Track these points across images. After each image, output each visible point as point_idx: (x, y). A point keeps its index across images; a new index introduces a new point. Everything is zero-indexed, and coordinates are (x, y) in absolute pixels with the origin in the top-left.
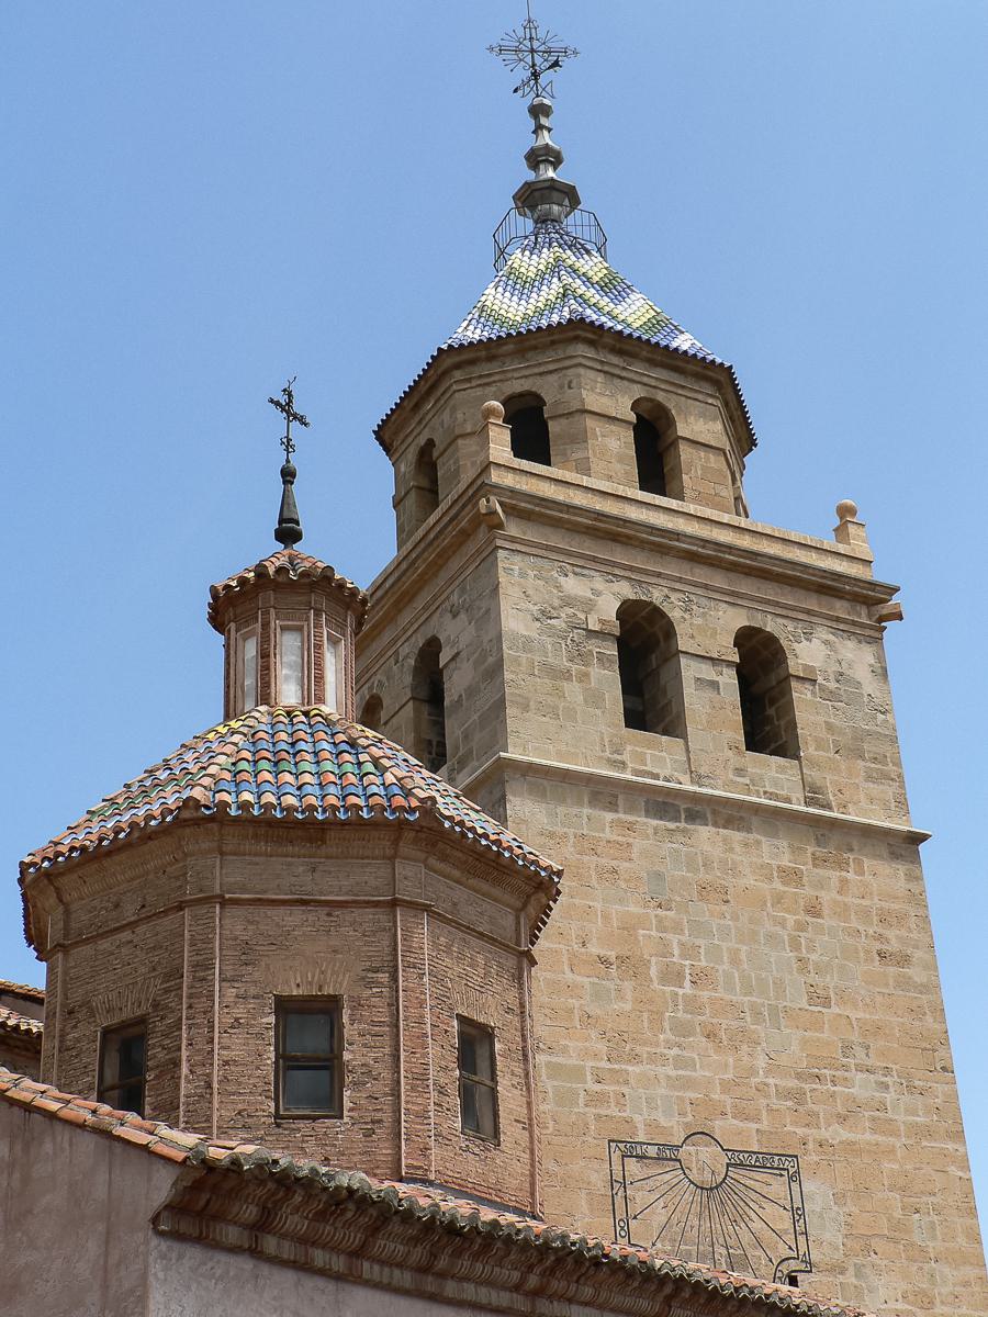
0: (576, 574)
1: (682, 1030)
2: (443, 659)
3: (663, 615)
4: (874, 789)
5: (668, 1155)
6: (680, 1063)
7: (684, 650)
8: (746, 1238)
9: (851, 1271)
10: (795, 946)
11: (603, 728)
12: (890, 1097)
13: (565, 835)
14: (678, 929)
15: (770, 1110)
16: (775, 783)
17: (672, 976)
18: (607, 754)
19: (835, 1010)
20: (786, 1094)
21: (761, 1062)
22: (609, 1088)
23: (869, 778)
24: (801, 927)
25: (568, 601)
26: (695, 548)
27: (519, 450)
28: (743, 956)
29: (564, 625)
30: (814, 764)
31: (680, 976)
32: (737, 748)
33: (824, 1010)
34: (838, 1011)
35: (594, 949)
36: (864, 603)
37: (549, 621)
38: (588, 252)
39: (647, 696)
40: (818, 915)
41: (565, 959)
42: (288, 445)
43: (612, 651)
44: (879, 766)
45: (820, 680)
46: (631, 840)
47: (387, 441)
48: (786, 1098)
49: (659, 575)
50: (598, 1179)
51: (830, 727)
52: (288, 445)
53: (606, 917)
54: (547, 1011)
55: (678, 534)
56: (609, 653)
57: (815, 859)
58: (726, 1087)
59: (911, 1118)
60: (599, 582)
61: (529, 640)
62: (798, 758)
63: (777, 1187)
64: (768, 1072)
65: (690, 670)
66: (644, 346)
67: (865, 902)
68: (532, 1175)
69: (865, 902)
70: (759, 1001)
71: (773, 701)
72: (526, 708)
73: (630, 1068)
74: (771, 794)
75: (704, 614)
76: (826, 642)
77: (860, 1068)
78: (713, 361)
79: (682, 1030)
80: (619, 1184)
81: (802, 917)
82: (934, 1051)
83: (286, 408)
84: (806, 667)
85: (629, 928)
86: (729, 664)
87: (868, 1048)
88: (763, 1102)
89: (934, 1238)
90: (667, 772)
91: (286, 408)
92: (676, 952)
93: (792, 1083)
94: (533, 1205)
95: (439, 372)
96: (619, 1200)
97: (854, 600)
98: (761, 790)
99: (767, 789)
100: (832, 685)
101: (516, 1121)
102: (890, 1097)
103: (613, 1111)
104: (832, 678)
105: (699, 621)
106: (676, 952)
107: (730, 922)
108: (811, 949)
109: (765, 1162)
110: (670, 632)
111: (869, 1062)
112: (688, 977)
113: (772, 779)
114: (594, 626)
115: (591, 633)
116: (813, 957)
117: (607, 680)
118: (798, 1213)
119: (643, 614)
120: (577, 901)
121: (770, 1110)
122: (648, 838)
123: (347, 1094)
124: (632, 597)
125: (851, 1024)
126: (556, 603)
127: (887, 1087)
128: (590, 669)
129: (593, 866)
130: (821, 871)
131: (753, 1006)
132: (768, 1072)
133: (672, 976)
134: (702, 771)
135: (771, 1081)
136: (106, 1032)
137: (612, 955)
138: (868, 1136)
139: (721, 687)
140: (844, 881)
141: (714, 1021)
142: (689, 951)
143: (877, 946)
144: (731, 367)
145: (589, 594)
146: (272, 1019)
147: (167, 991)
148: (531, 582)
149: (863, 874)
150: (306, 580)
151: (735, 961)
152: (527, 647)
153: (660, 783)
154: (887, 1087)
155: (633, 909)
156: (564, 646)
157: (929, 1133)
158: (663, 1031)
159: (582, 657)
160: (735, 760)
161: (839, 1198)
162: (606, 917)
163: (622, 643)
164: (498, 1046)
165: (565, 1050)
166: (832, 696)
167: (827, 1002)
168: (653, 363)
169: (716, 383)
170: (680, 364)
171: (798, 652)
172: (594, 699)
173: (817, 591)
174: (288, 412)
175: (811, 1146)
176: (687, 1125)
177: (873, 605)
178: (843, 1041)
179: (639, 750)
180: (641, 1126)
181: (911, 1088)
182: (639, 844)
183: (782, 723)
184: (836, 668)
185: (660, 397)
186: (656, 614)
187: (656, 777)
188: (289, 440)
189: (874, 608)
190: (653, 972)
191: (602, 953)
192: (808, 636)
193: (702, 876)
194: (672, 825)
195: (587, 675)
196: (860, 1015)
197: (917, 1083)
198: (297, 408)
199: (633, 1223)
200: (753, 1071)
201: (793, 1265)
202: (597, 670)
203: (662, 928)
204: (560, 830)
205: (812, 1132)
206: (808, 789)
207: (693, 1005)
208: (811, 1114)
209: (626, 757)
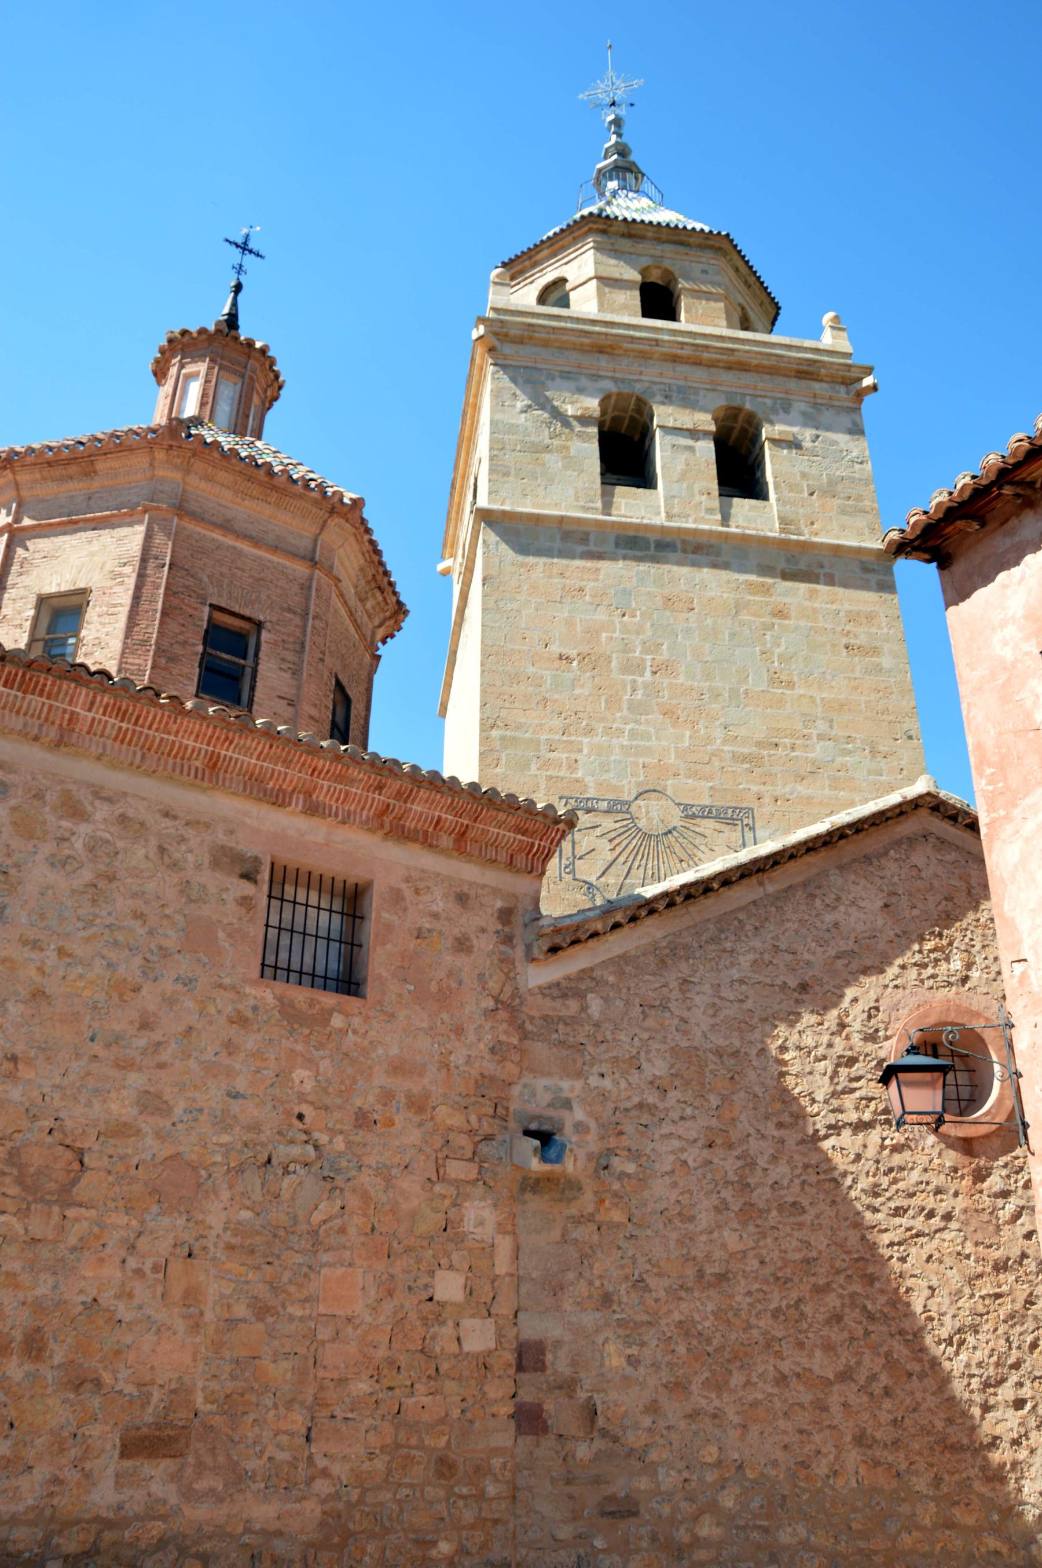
0: (561, 377)
1: (637, 709)
5: (618, 807)
6: (633, 735)
17: (633, 667)
19: (799, 691)
20: (745, 759)
21: (718, 733)
23: (843, 512)
33: (788, 692)
34: (802, 692)
35: (555, 649)
36: (843, 383)
42: (240, 269)
43: (594, 430)
48: (743, 762)
51: (804, 475)
52: (240, 269)
53: (570, 623)
64: (725, 742)
66: (650, 228)
73: (586, 740)
81: (767, 619)
83: (244, 247)
85: (592, 633)
86: (706, 434)
87: (831, 721)
91: (244, 247)
92: (639, 649)
101: (280, 697)
111: (834, 732)
112: (649, 669)
119: (632, 407)
125: (814, 702)
131: (710, 689)
132: (725, 742)
133: (633, 667)
135: (726, 748)
137: (573, 653)
141: (674, 702)
143: (844, 641)
144: (728, 235)
146: (31, 613)
150: (204, 337)
158: (620, 710)
164: (265, 635)
167: (790, 684)
168: (659, 240)
169: (718, 250)
170: (683, 238)
172: (571, 463)
174: (244, 249)
175: (766, 800)
176: (638, 784)
180: (591, 784)
188: (241, 266)
189: (851, 387)
190: (614, 664)
191: (565, 651)
195: (567, 448)
196: (825, 695)
197: (881, 748)
198: (251, 246)
199: (577, 862)
200: (709, 740)
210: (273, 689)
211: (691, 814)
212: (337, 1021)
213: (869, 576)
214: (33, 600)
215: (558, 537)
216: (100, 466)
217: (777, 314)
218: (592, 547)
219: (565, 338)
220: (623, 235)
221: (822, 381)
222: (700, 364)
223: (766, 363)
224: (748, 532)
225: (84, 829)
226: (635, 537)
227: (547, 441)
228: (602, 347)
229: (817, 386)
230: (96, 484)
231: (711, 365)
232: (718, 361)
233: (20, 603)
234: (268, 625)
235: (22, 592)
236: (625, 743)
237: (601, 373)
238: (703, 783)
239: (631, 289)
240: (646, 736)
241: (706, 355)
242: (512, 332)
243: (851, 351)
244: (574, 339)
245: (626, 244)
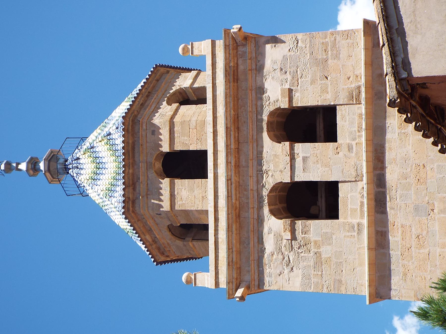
4: (344, 54)
7: (290, 179)
13: (403, 266)
18: (355, 234)
23: (337, 57)
26: (233, 168)
29: (292, 253)
32: (337, 148)
36: (237, 49)
37: (291, 262)
43: (299, 224)
44: (329, 48)
45: (287, 86)
46: (400, 226)
51: (313, 82)
55: (228, 180)
56: (301, 227)
61: (304, 276)
66: (127, 172)
74: (359, 127)
78: (123, 129)
84: (283, 96)
86: (292, 148)
90: (359, 196)
97: (237, 56)
98: (358, 134)
99: (356, 129)
104: (285, 77)
107: (435, 165)
114: (288, 236)
115: (294, 238)
120: (438, 264)
128: (312, 240)
129: (417, 251)
134: (354, 174)
139: (305, 155)
145: (272, 235)
153: (365, 201)
156: (302, 254)
166: (295, 79)
171: (275, 99)
173: (237, 82)
177: (237, 43)
179: (349, 212)
195: (316, 242)
202: (311, 235)
206: (351, 102)
215: (382, 251)
217: (162, 66)
219: (234, 241)
220: (134, 189)
221: (237, 64)
222: (238, 149)
223: (232, 105)
224: (364, 126)
226: (376, 201)
227: (312, 254)
228: (236, 216)
229: (241, 68)
231: (238, 142)
232: (235, 137)
237: (256, 216)
239: (174, 184)
241: (233, 146)
242: (235, 276)
243: (210, 41)
244: (234, 235)
245: (142, 187)
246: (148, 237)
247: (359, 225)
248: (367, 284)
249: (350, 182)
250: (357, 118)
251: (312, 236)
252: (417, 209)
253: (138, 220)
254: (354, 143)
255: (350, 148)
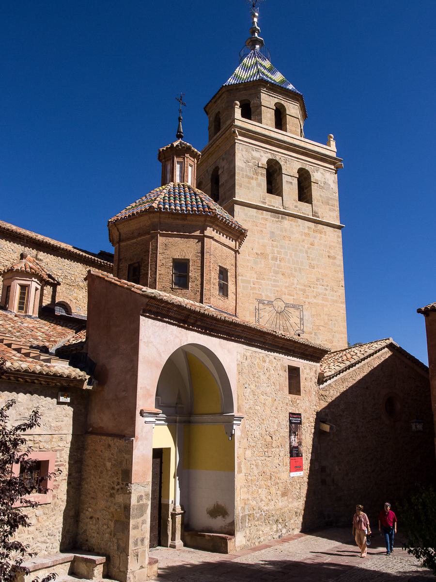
1: (276, 273)
2: (220, 172)
3: (279, 163)
5: (270, 303)
6: (275, 281)
8: (288, 324)
9: (314, 334)
10: (307, 253)
11: (261, 193)
12: (327, 292)
13: (249, 221)
14: (277, 247)
15: (297, 294)
16: (305, 210)
18: (262, 200)
19: (316, 270)
21: (296, 282)
22: (256, 286)
23: (330, 210)
24: (309, 248)
25: (253, 158)
27: (243, 115)
28: (293, 255)
30: (316, 206)
31: (276, 259)
35: (255, 251)
38: (266, 60)
39: (273, 185)
40: (313, 245)
41: (247, 253)
43: (265, 172)
47: (207, 111)
49: (278, 152)
50: (252, 308)
53: (258, 243)
54: (242, 266)
57: (314, 231)
58: (286, 287)
59: (331, 298)
60: (262, 154)
62: (312, 204)
63: (297, 313)
65: (285, 178)
67: (326, 243)
68: (236, 306)
69: (326, 243)
70: (297, 266)
71: (306, 189)
72: (241, 187)
73: (262, 281)
75: (290, 164)
76: (322, 173)
77: (320, 284)
79: (276, 273)
80: (257, 310)
82: (340, 281)
87: (323, 280)
88: (295, 292)
89: (335, 327)
92: (276, 252)
93: (303, 287)
94: (236, 314)
95: (222, 92)
96: (257, 314)
100: (322, 185)
102: (327, 292)
103: (257, 292)
105: (288, 165)
106: (276, 252)
108: (311, 254)
109: (294, 306)
110: (280, 168)
111: (323, 283)
113: (304, 209)
116: (311, 256)
117: (263, 180)
118: (302, 319)
121: (297, 294)
122: (270, 222)
123: (190, 284)
124: (271, 158)
126: (250, 158)
127: (327, 290)
130: (316, 234)
134: (286, 206)
136: (130, 266)
138: (321, 302)
140: (321, 237)
142: (279, 253)
143: (328, 254)
147: (145, 256)
148: (244, 153)
149: (326, 235)
151: (291, 256)
152: (242, 169)
153: (275, 208)
154: (327, 290)
155: (266, 241)
157: (336, 301)
159: (256, 173)
160: (295, 204)
161: (313, 316)
162: (258, 243)
163: (268, 171)
165: (246, 276)
166: (322, 188)
172: (259, 185)
178: (317, 277)
181: (333, 290)
182: (268, 224)
183: (309, 194)
184: (324, 180)
185: (282, 102)
186: (277, 163)
187: (274, 207)
192: (317, 171)
193: (284, 234)
194: (277, 220)
195: (257, 178)
200: (293, 284)
201: (299, 332)
203: (273, 246)
204: (248, 219)
205: (307, 300)
207: (279, 267)
208: (307, 295)
209: (266, 201)
210: (231, 290)
211: (287, 306)
212: (298, 402)
213: (335, 233)
214: (171, 259)
216: (188, 218)
218: (264, 216)
225: (266, 364)
230: (186, 222)
233: (167, 260)
234: (229, 270)
235: (167, 256)
236: (273, 283)
238: (291, 297)
240: (278, 281)
246: (242, 86)
247: (266, 202)
248: (243, 201)
249: (283, 203)
250: (307, 213)
251: (260, 177)
252: (273, 233)
253: (254, 85)
254: (298, 209)
255: (296, 207)
